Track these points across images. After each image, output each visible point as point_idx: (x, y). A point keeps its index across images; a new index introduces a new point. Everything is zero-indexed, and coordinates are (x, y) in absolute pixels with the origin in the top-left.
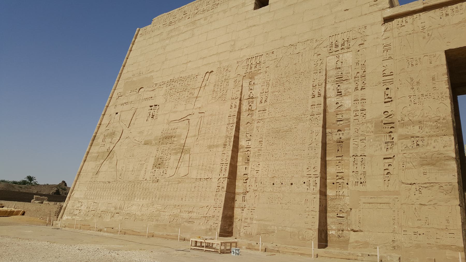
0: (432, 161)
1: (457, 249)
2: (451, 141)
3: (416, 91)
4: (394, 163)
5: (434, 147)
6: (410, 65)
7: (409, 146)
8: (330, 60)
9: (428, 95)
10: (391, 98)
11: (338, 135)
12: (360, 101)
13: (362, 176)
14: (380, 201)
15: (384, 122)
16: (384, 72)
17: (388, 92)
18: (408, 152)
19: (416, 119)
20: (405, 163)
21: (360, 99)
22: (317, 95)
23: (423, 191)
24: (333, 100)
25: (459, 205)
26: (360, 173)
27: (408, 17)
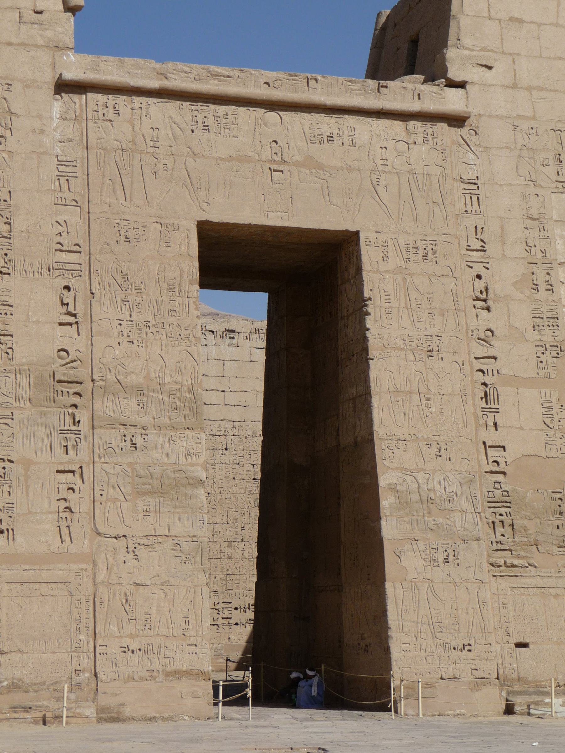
5: (168, 455)
6: (123, 238)
7: (114, 444)
10: (75, 315)
14: (45, 576)
17: (68, 297)
18: (114, 459)
20: (105, 488)
23: (142, 552)
27: (122, 98)
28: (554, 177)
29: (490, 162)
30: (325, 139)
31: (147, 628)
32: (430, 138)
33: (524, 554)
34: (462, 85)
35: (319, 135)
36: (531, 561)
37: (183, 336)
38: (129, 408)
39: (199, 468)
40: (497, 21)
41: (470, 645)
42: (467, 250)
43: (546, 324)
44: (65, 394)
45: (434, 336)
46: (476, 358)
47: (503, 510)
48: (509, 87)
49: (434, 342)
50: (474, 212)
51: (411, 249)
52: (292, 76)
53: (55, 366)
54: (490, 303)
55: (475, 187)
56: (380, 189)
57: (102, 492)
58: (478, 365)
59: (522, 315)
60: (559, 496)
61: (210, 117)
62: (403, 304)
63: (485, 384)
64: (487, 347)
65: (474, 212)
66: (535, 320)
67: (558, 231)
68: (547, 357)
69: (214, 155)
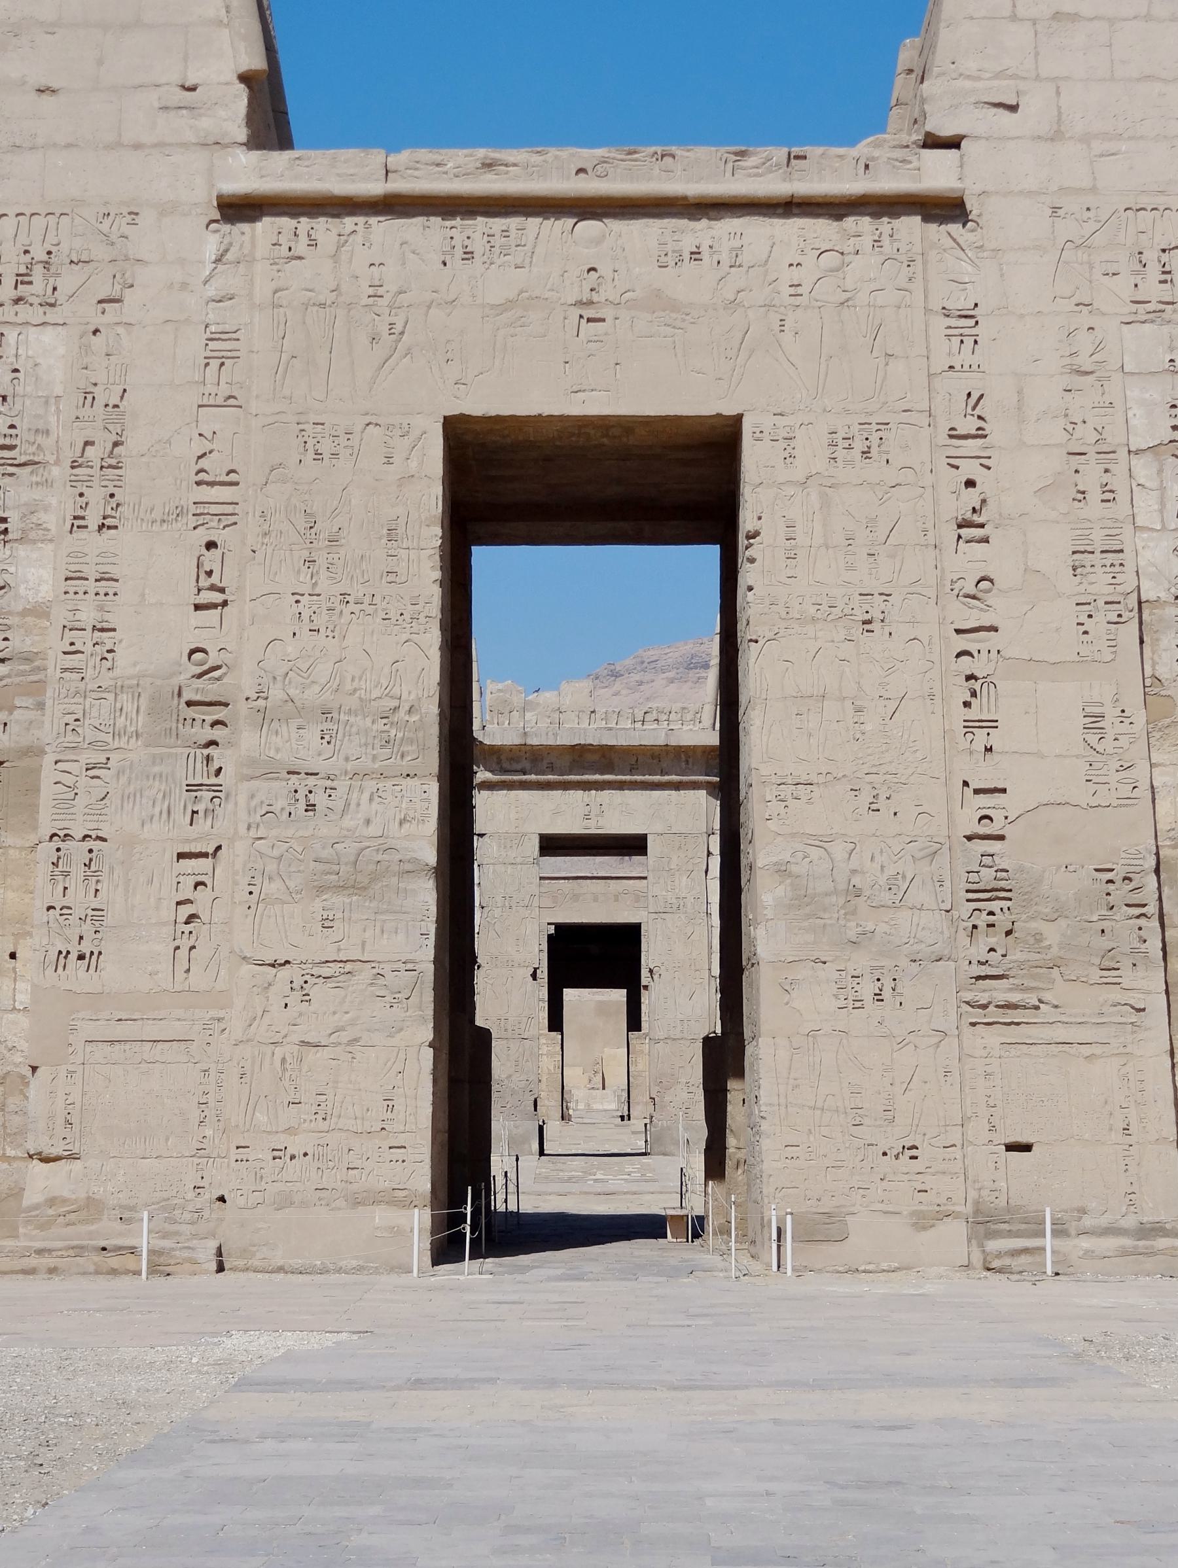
2: (427, 800)
3: (324, 574)
4: (222, 872)
6: (311, 454)
7: (276, 808)
9: (367, 600)
10: (222, 590)
12: (91, 586)
13: (87, 929)
14: (152, 1031)
15: (188, 695)
16: (203, 463)
17: (211, 559)
18: (274, 833)
19: (312, 696)
21: (91, 572)
23: (317, 991)
26: (78, 912)
28: (1128, 293)
29: (1002, 275)
30: (686, 256)
32: (886, 241)
33: (1028, 983)
34: (953, 143)
35: (674, 251)
36: (1047, 996)
37: (407, 616)
40: (1030, 23)
42: (951, 437)
43: (1098, 564)
45: (876, 595)
46: (958, 631)
47: (995, 906)
48: (1046, 140)
49: (876, 605)
50: (966, 368)
51: (840, 441)
52: (630, 153)
53: (182, 679)
55: (972, 322)
57: (251, 888)
59: (1051, 548)
60: (1109, 876)
61: (477, 236)
64: (981, 610)
66: (1076, 556)
67: (1133, 393)
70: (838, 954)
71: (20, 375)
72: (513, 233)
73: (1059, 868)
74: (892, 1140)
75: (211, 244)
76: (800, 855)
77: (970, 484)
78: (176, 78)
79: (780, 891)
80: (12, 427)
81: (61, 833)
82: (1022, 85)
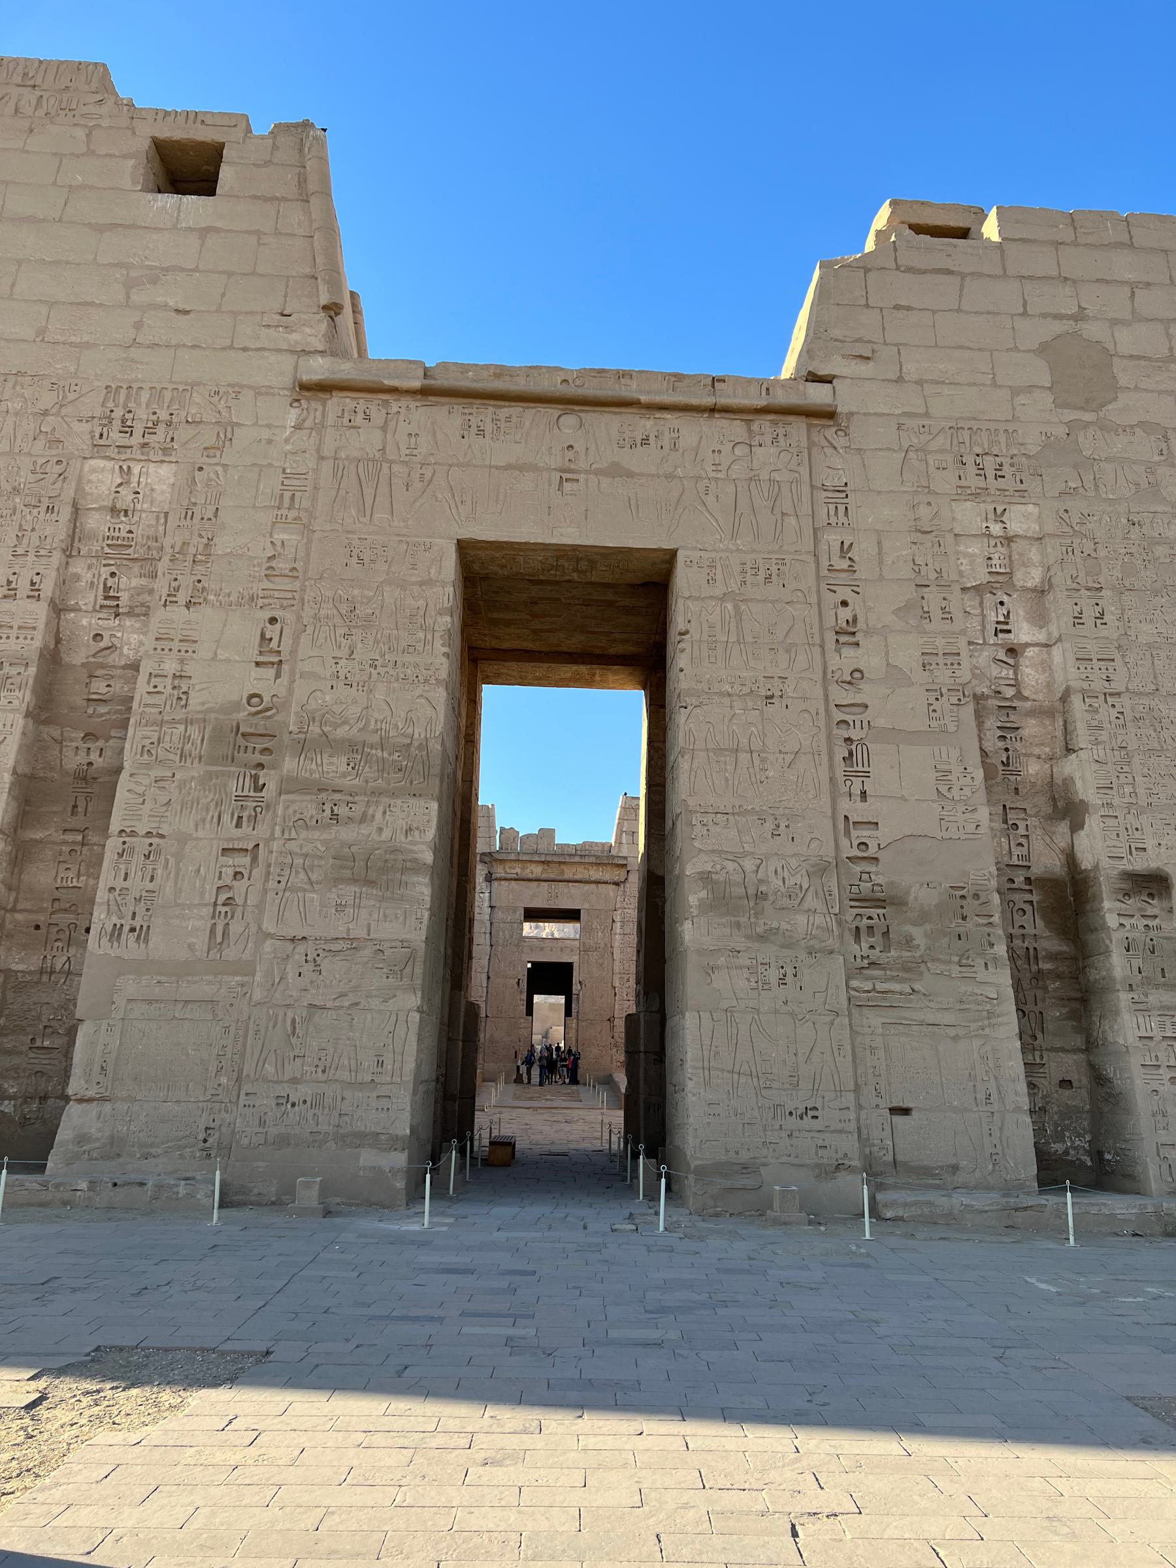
0: (371, 872)
1: (393, 1143)
8: (93, 471)
11: (82, 753)
12: (176, 645)
13: (141, 909)
16: (273, 564)
17: (272, 631)
19: (342, 732)
22: (23, 587)
24: (84, 622)
25: (419, 1010)
30: (639, 442)
31: (320, 1070)
32: (781, 439)
36: (917, 987)
38: (334, 767)
39: (424, 847)
41: (816, 1109)
44: (250, 750)
47: (873, 912)
54: (859, 637)
55: (844, 495)
56: (710, 500)
58: (839, 716)
62: (733, 638)
63: (848, 740)
65: (840, 524)
68: (944, 704)
69: (487, 463)
70: (750, 945)
71: (140, 496)
72: (514, 419)
73: (922, 885)
74: (797, 1103)
75: (292, 416)
76: (718, 867)
77: (844, 604)
78: (277, 307)
79: (703, 894)
80: (130, 532)
81: (128, 830)
82: (875, 347)
